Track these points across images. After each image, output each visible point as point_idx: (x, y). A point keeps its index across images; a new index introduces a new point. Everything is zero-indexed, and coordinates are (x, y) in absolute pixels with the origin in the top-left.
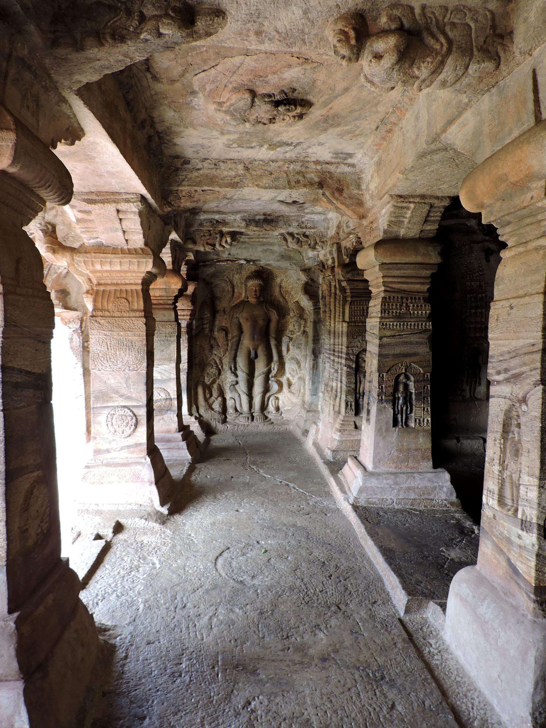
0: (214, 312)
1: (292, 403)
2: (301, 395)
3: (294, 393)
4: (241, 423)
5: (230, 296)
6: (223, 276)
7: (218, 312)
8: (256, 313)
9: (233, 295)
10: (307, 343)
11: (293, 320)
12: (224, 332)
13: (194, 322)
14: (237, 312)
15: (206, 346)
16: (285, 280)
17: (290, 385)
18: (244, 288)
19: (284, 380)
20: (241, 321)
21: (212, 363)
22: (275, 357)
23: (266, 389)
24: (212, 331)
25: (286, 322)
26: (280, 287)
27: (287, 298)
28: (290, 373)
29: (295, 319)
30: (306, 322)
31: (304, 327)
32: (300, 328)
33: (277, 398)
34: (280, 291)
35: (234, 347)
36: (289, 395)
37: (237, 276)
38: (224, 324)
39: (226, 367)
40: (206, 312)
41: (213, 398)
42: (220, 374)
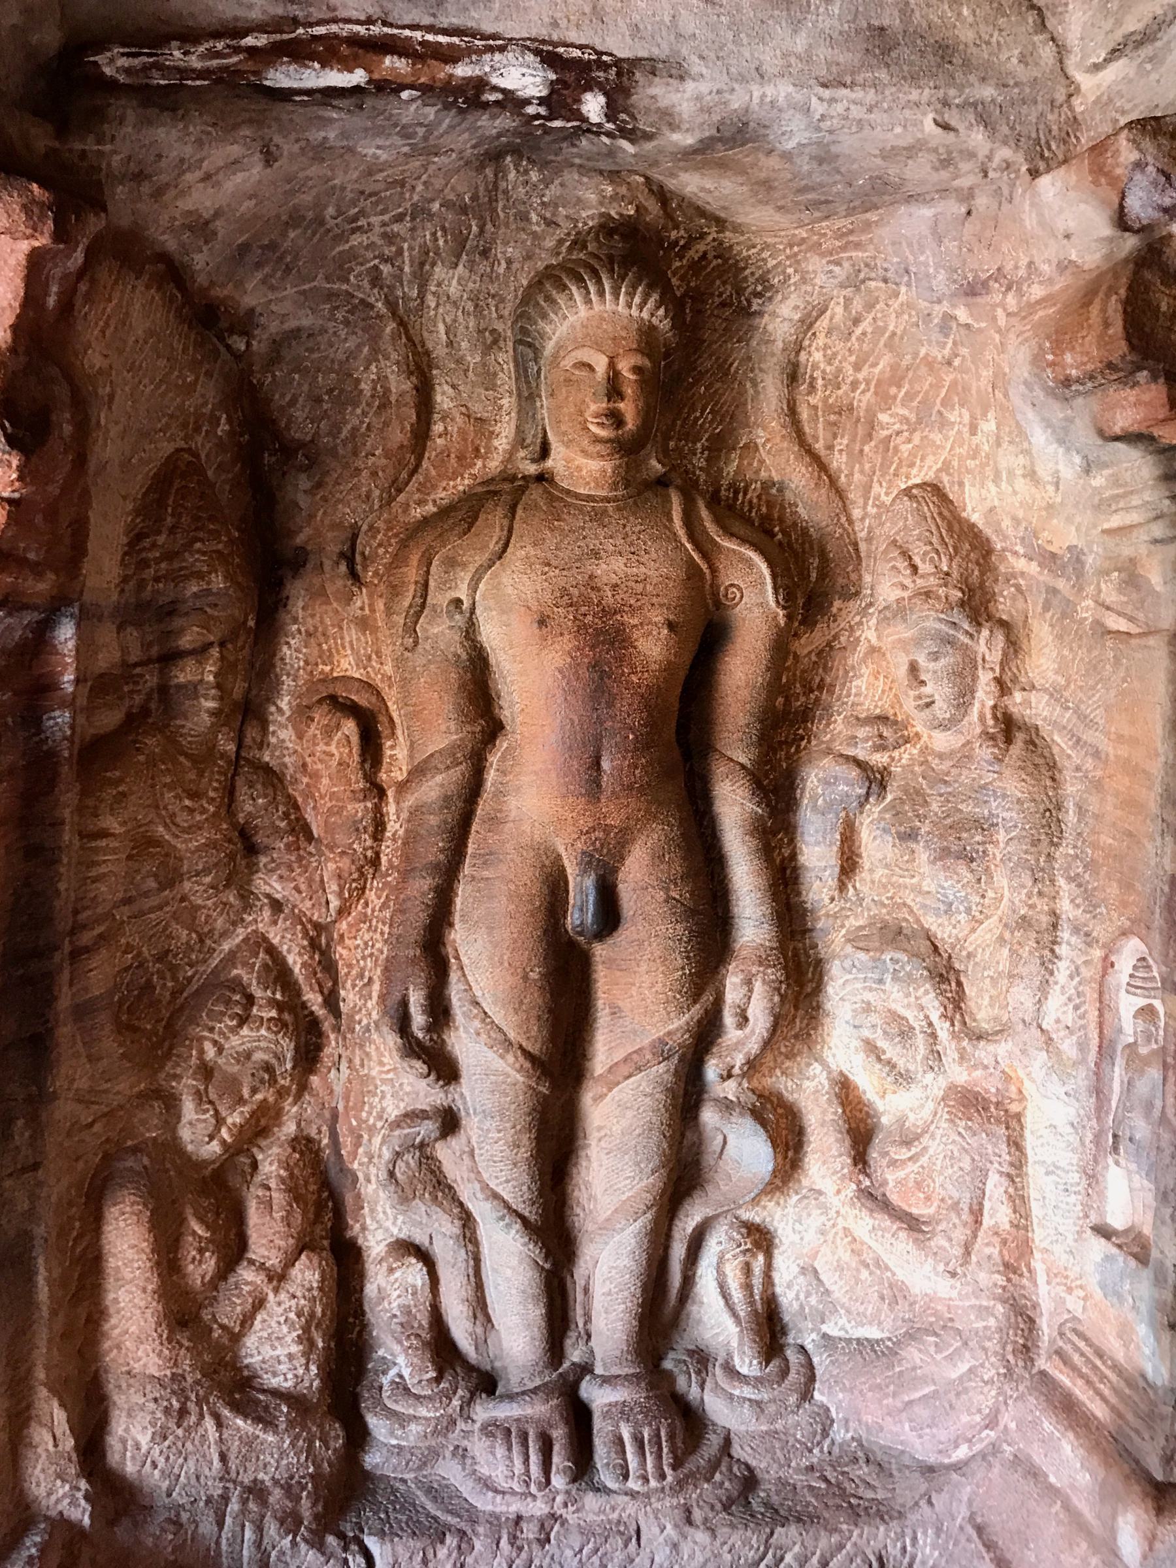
0: (271, 570)
1: (896, 1294)
2: (987, 1249)
3: (912, 1224)
4: (484, 1503)
5: (399, 436)
6: (341, 268)
7: (298, 562)
8: (611, 568)
9: (421, 435)
10: (1049, 819)
11: (901, 631)
12: (350, 727)
13: (66, 634)
14: (451, 563)
15: (193, 840)
16: (837, 311)
17: (860, 1135)
18: (506, 379)
19: (809, 1091)
20: (490, 634)
21: (248, 976)
22: (752, 922)
23: (683, 1172)
24: (248, 711)
25: (826, 653)
26: (793, 375)
27: (838, 461)
28: (871, 1048)
29: (931, 619)
30: (1014, 646)
31: (1003, 687)
32: (964, 696)
33: (761, 1239)
34: (792, 411)
35: (434, 850)
36: (864, 1224)
37: (451, 280)
38: (346, 665)
39: (363, 1003)
40: (195, 560)
41: (247, 1275)
42: (309, 1056)
